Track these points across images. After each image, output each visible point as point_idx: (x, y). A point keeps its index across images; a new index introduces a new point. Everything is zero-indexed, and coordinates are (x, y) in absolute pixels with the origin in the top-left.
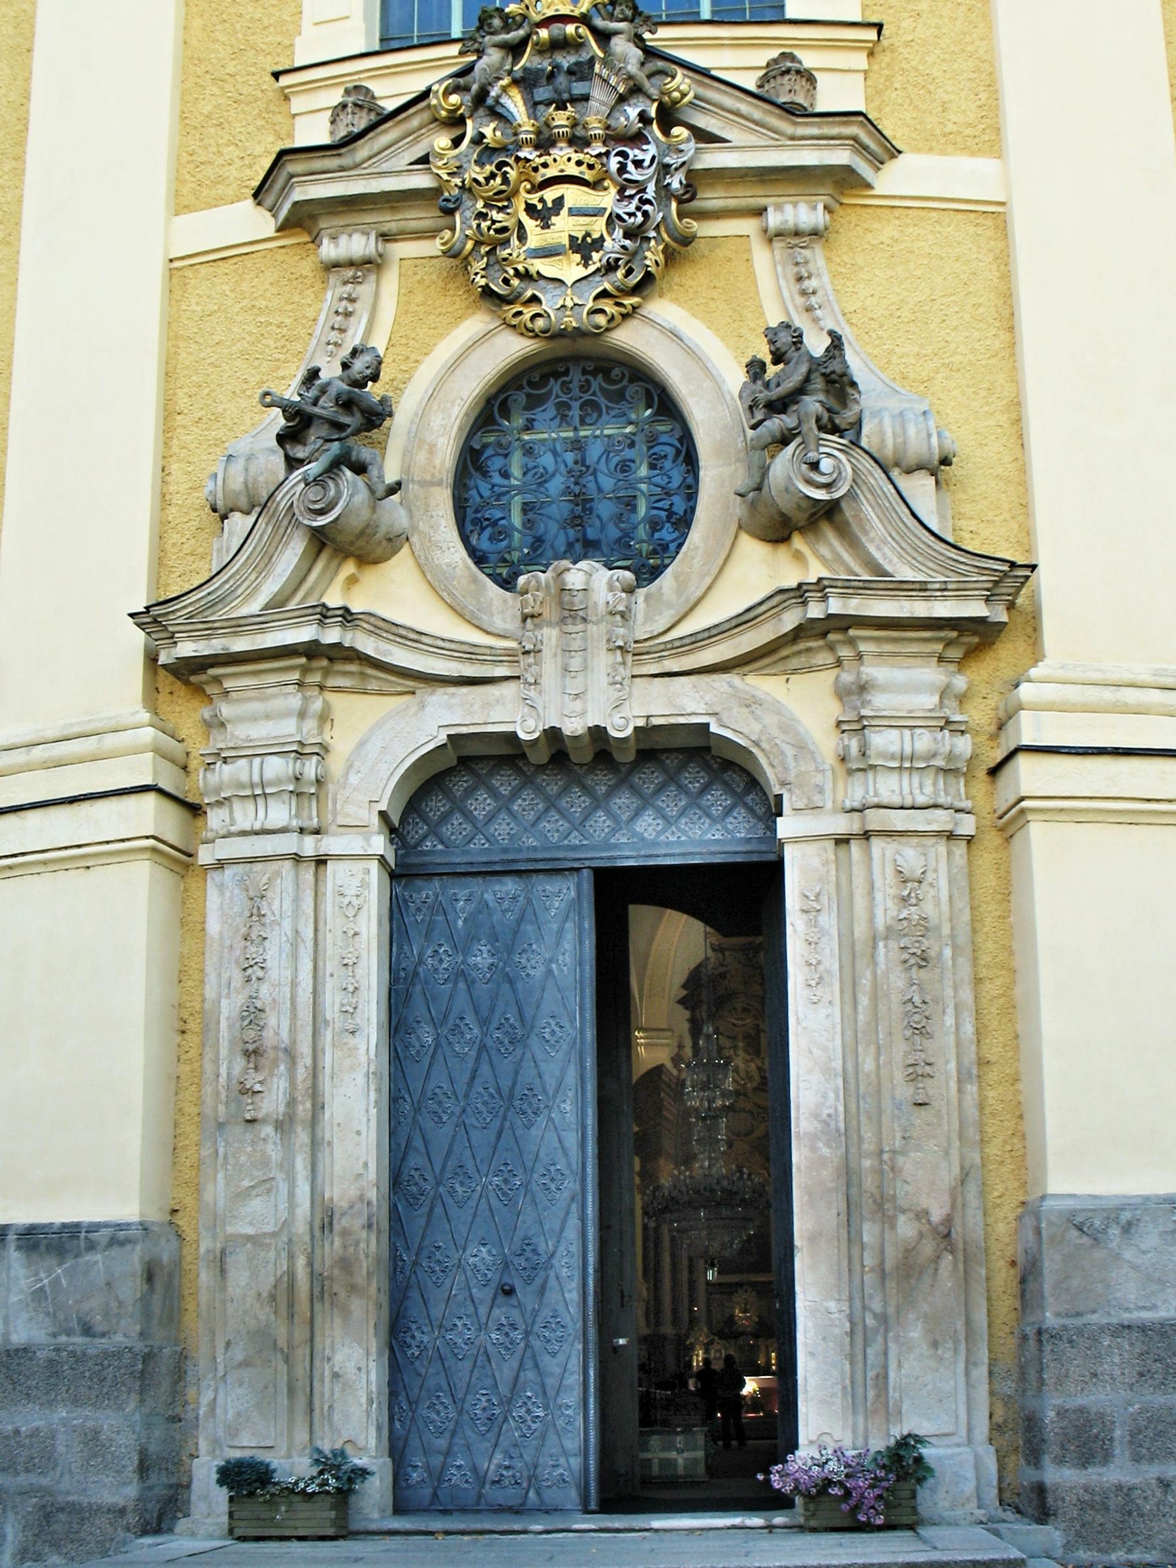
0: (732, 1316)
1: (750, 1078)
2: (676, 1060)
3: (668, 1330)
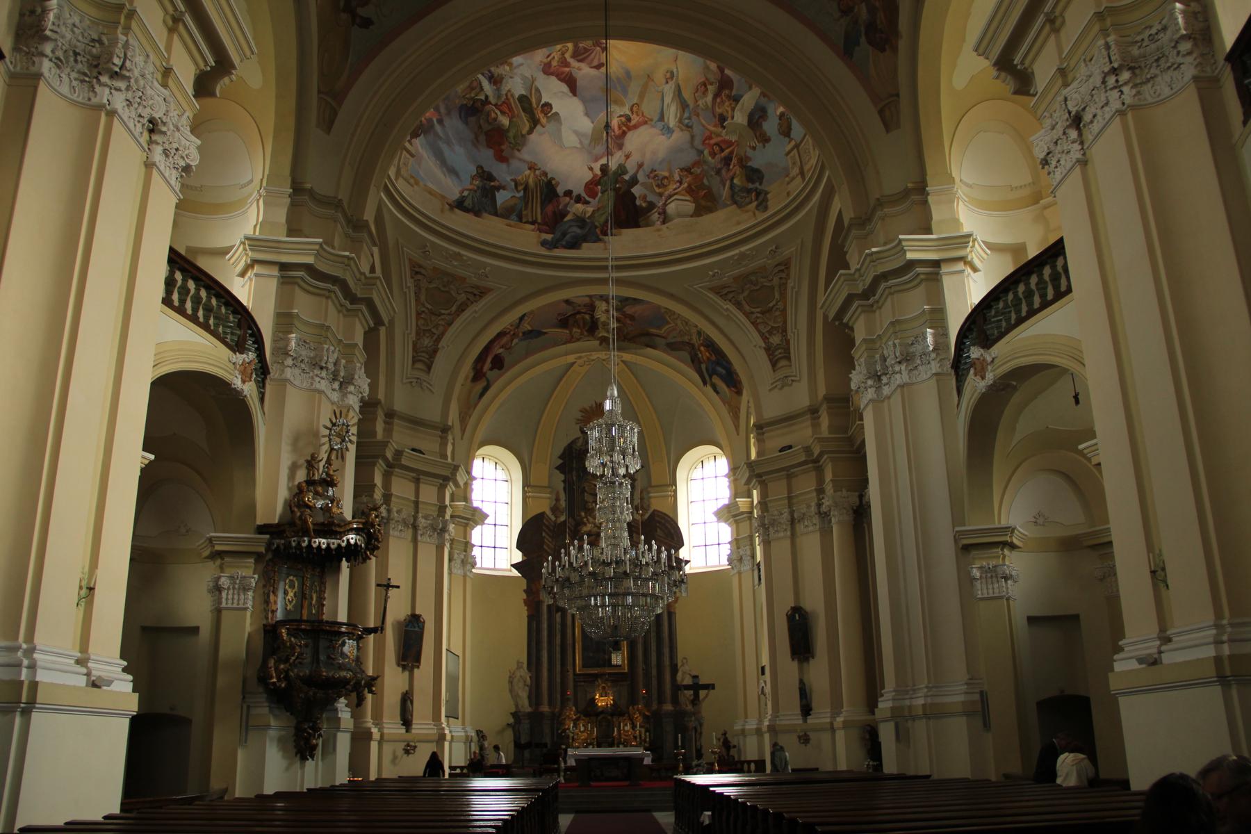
0: (594, 699)
2: (555, 510)
3: (545, 709)
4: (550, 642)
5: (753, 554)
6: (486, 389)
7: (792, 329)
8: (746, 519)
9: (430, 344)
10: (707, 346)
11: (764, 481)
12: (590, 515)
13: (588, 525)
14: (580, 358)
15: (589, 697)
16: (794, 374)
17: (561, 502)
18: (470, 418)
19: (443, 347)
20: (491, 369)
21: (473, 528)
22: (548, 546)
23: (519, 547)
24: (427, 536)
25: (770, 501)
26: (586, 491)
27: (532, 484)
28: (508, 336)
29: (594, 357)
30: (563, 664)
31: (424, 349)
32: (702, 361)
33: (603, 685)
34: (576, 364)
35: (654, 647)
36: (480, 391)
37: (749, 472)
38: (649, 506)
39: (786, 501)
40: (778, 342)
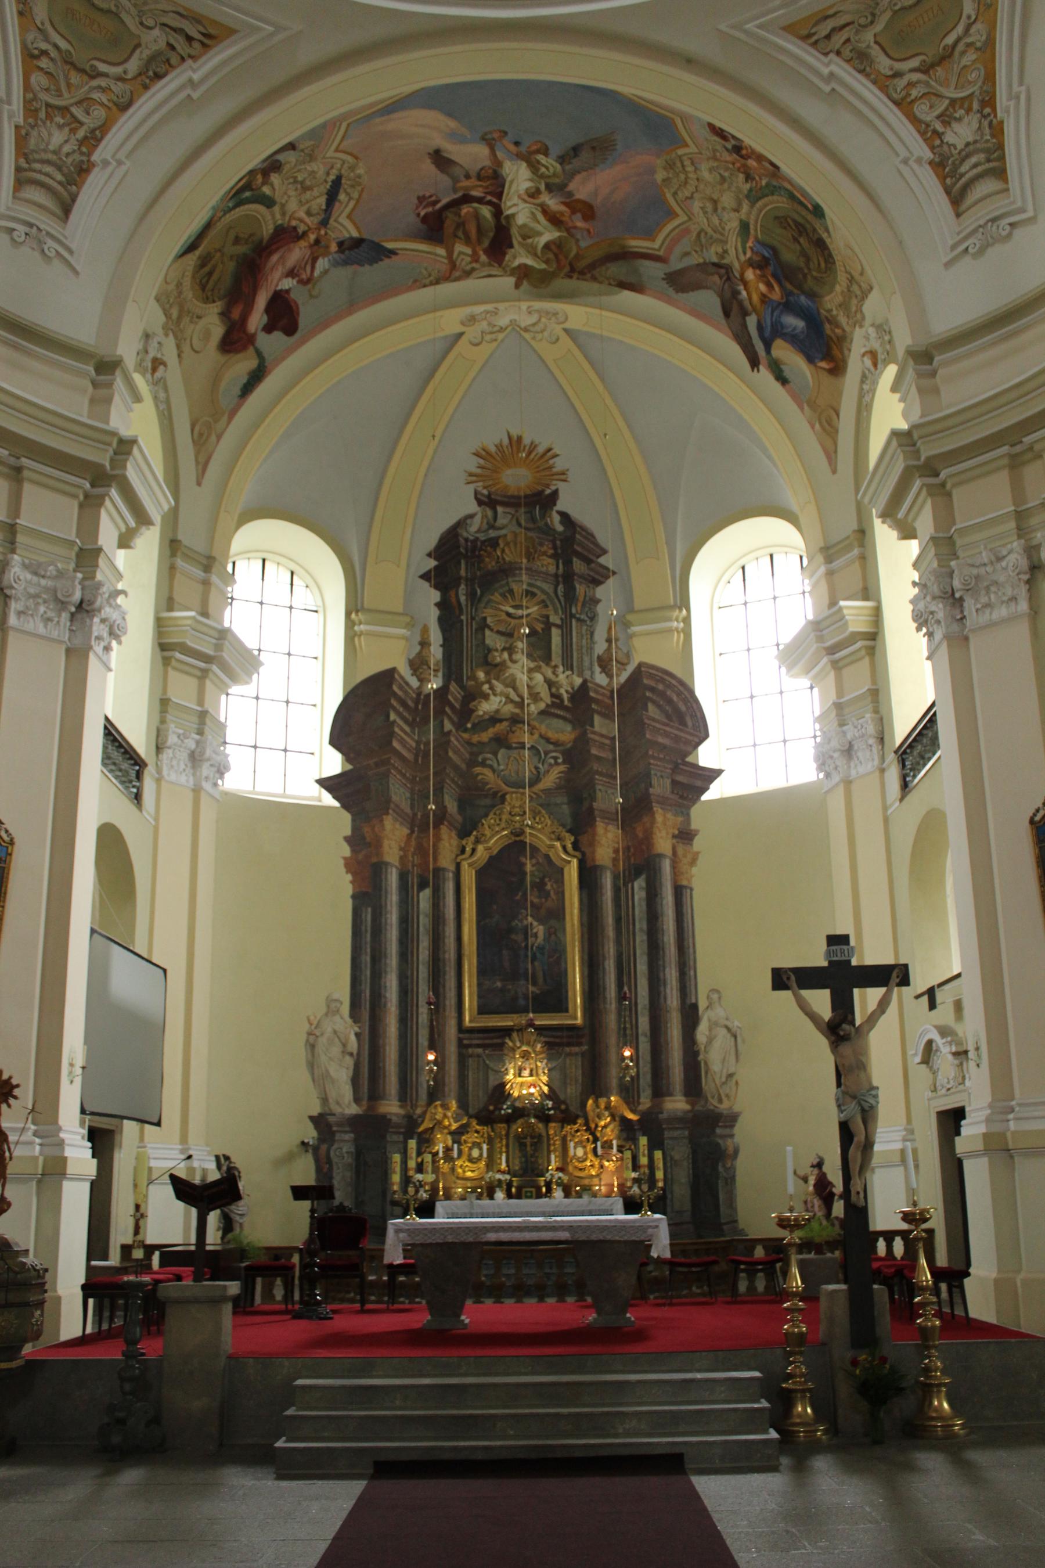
0: (503, 1085)
1: (535, 697)
2: (418, 665)
3: (391, 1107)
4: (405, 955)
5: (882, 732)
6: (256, 377)
7: (1010, 85)
8: (863, 652)
9: (67, 149)
10: (760, 264)
11: (943, 485)
12: (497, 679)
13: (492, 697)
14: (472, 319)
15: (493, 1082)
16: (1019, 204)
17: (432, 648)
18: (219, 437)
19: (106, 163)
20: (268, 329)
22: (402, 742)
23: (336, 741)
24: (38, 619)
25: (963, 531)
27: (366, 605)
28: (303, 243)
29: (503, 321)
30: (437, 1007)
31: (50, 156)
32: (749, 308)
33: (524, 1048)
34: (464, 338)
35: (642, 967)
36: (245, 381)
37: (905, 459)
38: (628, 655)
39: (1013, 524)
40: (970, 139)
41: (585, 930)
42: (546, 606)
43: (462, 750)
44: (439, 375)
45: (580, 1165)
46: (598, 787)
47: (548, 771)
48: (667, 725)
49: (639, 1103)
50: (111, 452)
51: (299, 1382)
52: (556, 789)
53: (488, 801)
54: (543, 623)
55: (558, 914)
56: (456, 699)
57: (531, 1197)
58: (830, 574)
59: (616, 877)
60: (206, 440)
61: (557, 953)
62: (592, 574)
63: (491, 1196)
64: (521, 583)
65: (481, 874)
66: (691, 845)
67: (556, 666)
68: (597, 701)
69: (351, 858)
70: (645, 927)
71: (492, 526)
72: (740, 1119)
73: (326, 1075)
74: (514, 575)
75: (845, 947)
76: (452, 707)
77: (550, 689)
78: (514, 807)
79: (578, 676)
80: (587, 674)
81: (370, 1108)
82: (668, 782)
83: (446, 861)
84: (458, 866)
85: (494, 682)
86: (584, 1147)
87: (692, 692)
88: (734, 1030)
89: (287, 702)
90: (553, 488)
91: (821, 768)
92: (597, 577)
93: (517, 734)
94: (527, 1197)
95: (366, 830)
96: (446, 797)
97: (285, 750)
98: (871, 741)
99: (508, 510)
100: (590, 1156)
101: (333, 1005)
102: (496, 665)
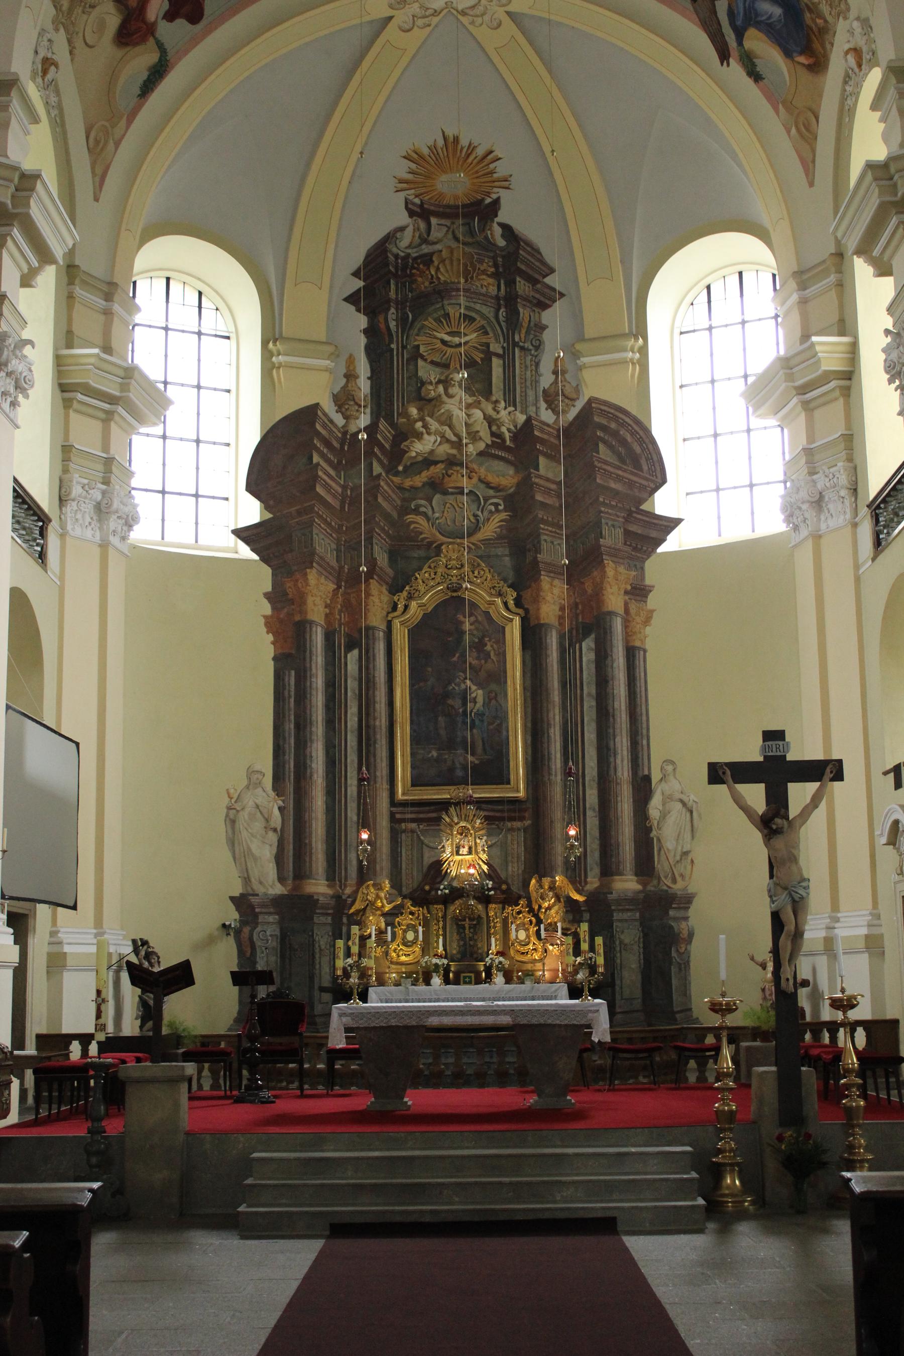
0: (439, 863)
1: (474, 436)
4: (330, 723)
6: (158, 73)
8: (837, 393)
12: (431, 417)
13: (426, 436)
15: (428, 859)
18: (117, 144)
20: (170, 16)
21: (130, 430)
22: (327, 487)
23: (254, 486)
26: (422, 357)
27: (284, 334)
33: (463, 824)
35: (590, 735)
36: (145, 78)
37: (880, 194)
38: (577, 389)
41: (528, 694)
42: (486, 333)
43: (394, 496)
44: (365, 64)
45: (522, 949)
46: (543, 537)
47: (488, 519)
48: (619, 468)
49: (586, 883)
50: (13, 189)
51: (255, 1155)
52: (496, 539)
53: (422, 553)
54: (482, 352)
55: (499, 677)
56: (385, 438)
57: (470, 983)
58: (803, 302)
59: (561, 637)
60: (102, 149)
61: (499, 719)
62: (537, 296)
63: (427, 982)
64: (457, 307)
65: (415, 633)
66: (645, 602)
67: (497, 402)
68: (542, 441)
69: (271, 616)
70: (594, 692)
71: (424, 241)
72: (696, 902)
73: (249, 853)
74: (450, 297)
75: (781, 743)
76: (381, 446)
77: (490, 427)
78: (450, 559)
79: (522, 413)
80: (532, 411)
81: (296, 888)
82: (620, 532)
83: (376, 617)
84: (389, 624)
85: (428, 419)
86: (527, 930)
87: (647, 432)
88: (690, 804)
89: (198, 441)
90: (494, 196)
91: (789, 518)
92: (542, 299)
93: (454, 477)
94: (465, 983)
95: (289, 585)
96: (376, 548)
97: (197, 496)
98: (843, 493)
99: (443, 221)
100: (533, 939)
101: (255, 777)
102: (430, 400)
